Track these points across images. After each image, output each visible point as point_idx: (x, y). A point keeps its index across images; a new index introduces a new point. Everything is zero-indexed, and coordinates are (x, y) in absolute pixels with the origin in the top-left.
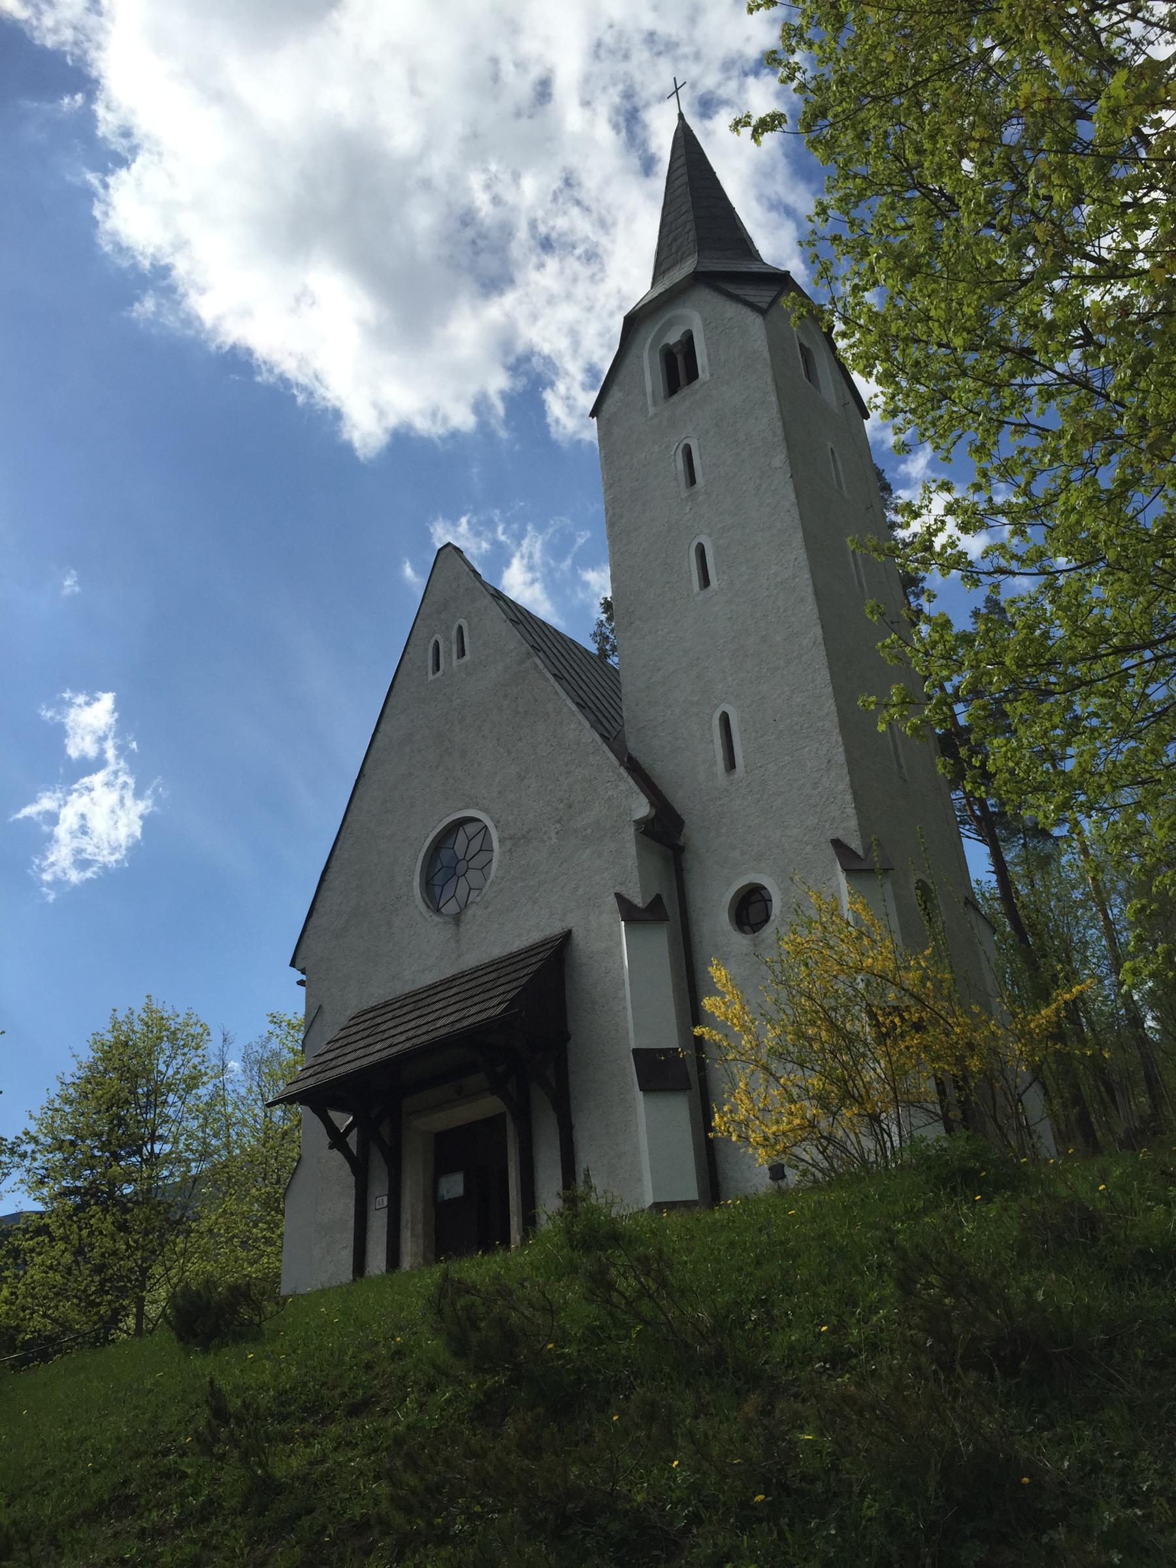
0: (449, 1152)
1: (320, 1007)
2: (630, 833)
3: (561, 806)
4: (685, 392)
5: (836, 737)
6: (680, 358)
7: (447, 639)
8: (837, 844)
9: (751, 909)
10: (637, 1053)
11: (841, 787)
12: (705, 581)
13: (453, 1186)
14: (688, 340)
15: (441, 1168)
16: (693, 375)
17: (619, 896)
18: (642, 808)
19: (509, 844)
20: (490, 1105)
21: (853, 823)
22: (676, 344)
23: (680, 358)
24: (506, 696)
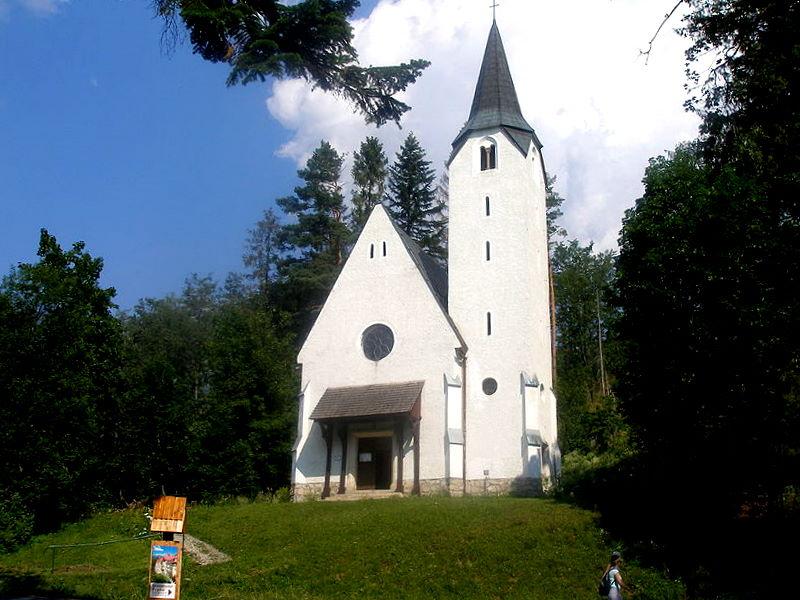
0: (364, 445)
4: (488, 171)
6: (488, 155)
9: (490, 386)
13: (367, 457)
14: (493, 148)
15: (361, 451)
16: (493, 166)
18: (459, 346)
23: (488, 155)
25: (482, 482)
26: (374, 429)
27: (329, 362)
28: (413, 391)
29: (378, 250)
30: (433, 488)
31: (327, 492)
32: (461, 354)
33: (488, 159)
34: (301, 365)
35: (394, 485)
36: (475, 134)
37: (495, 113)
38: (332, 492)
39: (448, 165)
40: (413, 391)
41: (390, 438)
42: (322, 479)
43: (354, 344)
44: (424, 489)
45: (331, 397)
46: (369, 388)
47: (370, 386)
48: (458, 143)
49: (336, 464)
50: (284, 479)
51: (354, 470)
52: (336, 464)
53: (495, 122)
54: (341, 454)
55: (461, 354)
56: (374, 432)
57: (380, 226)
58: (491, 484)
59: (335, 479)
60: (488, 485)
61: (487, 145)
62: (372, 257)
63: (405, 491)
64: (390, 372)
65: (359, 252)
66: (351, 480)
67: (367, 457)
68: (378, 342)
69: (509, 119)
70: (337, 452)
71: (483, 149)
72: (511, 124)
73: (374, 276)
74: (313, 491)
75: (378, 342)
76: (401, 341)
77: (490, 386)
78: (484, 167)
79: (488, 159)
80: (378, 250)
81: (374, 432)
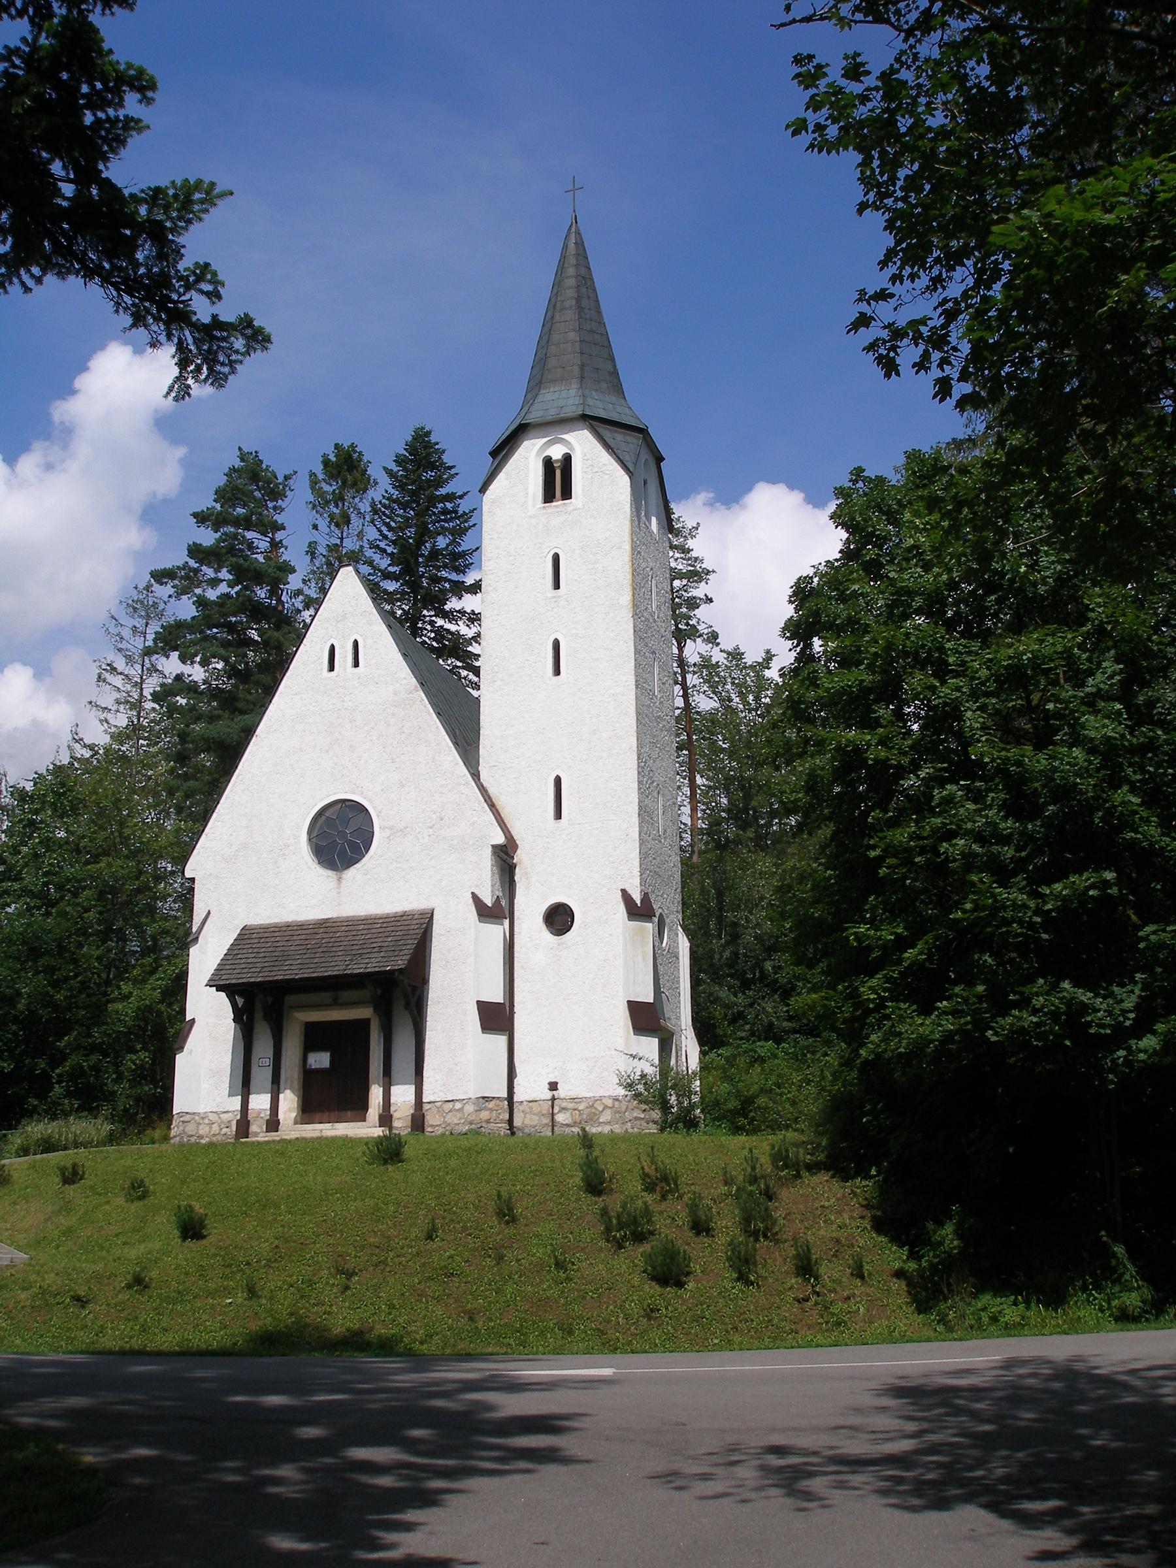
0: (315, 1037)
1: (209, 912)
2: (488, 852)
4: (558, 503)
5: (635, 820)
7: (342, 647)
8: (624, 892)
9: (559, 919)
10: (478, 1002)
14: (567, 459)
16: (567, 494)
17: (473, 893)
18: (500, 839)
19: (388, 832)
20: (364, 1013)
21: (637, 881)
22: (557, 461)
24: (393, 715)
25: (546, 1107)
26: (336, 1003)
27: (248, 874)
28: (417, 933)
29: (344, 657)
30: (452, 1119)
31: (243, 1126)
32: (505, 858)
33: (557, 481)
34: (193, 880)
36: (533, 433)
37: (573, 392)
38: (254, 1128)
39: (483, 489)
40: (417, 933)
42: (236, 1103)
45: (247, 937)
46: (325, 925)
47: (326, 921)
48: (503, 450)
51: (296, 1084)
53: (572, 410)
55: (505, 858)
56: (342, 1008)
58: (563, 1109)
59: (260, 1102)
60: (556, 1109)
62: (331, 668)
63: (396, 1124)
64: (369, 892)
65: (307, 658)
66: (289, 1102)
67: (321, 1060)
68: (341, 835)
69: (599, 404)
70: (263, 1050)
71: (548, 463)
72: (603, 415)
74: (215, 1128)
75: (341, 835)
76: (388, 832)
78: (549, 497)
79: (557, 481)
80: (344, 657)
81: (342, 1008)
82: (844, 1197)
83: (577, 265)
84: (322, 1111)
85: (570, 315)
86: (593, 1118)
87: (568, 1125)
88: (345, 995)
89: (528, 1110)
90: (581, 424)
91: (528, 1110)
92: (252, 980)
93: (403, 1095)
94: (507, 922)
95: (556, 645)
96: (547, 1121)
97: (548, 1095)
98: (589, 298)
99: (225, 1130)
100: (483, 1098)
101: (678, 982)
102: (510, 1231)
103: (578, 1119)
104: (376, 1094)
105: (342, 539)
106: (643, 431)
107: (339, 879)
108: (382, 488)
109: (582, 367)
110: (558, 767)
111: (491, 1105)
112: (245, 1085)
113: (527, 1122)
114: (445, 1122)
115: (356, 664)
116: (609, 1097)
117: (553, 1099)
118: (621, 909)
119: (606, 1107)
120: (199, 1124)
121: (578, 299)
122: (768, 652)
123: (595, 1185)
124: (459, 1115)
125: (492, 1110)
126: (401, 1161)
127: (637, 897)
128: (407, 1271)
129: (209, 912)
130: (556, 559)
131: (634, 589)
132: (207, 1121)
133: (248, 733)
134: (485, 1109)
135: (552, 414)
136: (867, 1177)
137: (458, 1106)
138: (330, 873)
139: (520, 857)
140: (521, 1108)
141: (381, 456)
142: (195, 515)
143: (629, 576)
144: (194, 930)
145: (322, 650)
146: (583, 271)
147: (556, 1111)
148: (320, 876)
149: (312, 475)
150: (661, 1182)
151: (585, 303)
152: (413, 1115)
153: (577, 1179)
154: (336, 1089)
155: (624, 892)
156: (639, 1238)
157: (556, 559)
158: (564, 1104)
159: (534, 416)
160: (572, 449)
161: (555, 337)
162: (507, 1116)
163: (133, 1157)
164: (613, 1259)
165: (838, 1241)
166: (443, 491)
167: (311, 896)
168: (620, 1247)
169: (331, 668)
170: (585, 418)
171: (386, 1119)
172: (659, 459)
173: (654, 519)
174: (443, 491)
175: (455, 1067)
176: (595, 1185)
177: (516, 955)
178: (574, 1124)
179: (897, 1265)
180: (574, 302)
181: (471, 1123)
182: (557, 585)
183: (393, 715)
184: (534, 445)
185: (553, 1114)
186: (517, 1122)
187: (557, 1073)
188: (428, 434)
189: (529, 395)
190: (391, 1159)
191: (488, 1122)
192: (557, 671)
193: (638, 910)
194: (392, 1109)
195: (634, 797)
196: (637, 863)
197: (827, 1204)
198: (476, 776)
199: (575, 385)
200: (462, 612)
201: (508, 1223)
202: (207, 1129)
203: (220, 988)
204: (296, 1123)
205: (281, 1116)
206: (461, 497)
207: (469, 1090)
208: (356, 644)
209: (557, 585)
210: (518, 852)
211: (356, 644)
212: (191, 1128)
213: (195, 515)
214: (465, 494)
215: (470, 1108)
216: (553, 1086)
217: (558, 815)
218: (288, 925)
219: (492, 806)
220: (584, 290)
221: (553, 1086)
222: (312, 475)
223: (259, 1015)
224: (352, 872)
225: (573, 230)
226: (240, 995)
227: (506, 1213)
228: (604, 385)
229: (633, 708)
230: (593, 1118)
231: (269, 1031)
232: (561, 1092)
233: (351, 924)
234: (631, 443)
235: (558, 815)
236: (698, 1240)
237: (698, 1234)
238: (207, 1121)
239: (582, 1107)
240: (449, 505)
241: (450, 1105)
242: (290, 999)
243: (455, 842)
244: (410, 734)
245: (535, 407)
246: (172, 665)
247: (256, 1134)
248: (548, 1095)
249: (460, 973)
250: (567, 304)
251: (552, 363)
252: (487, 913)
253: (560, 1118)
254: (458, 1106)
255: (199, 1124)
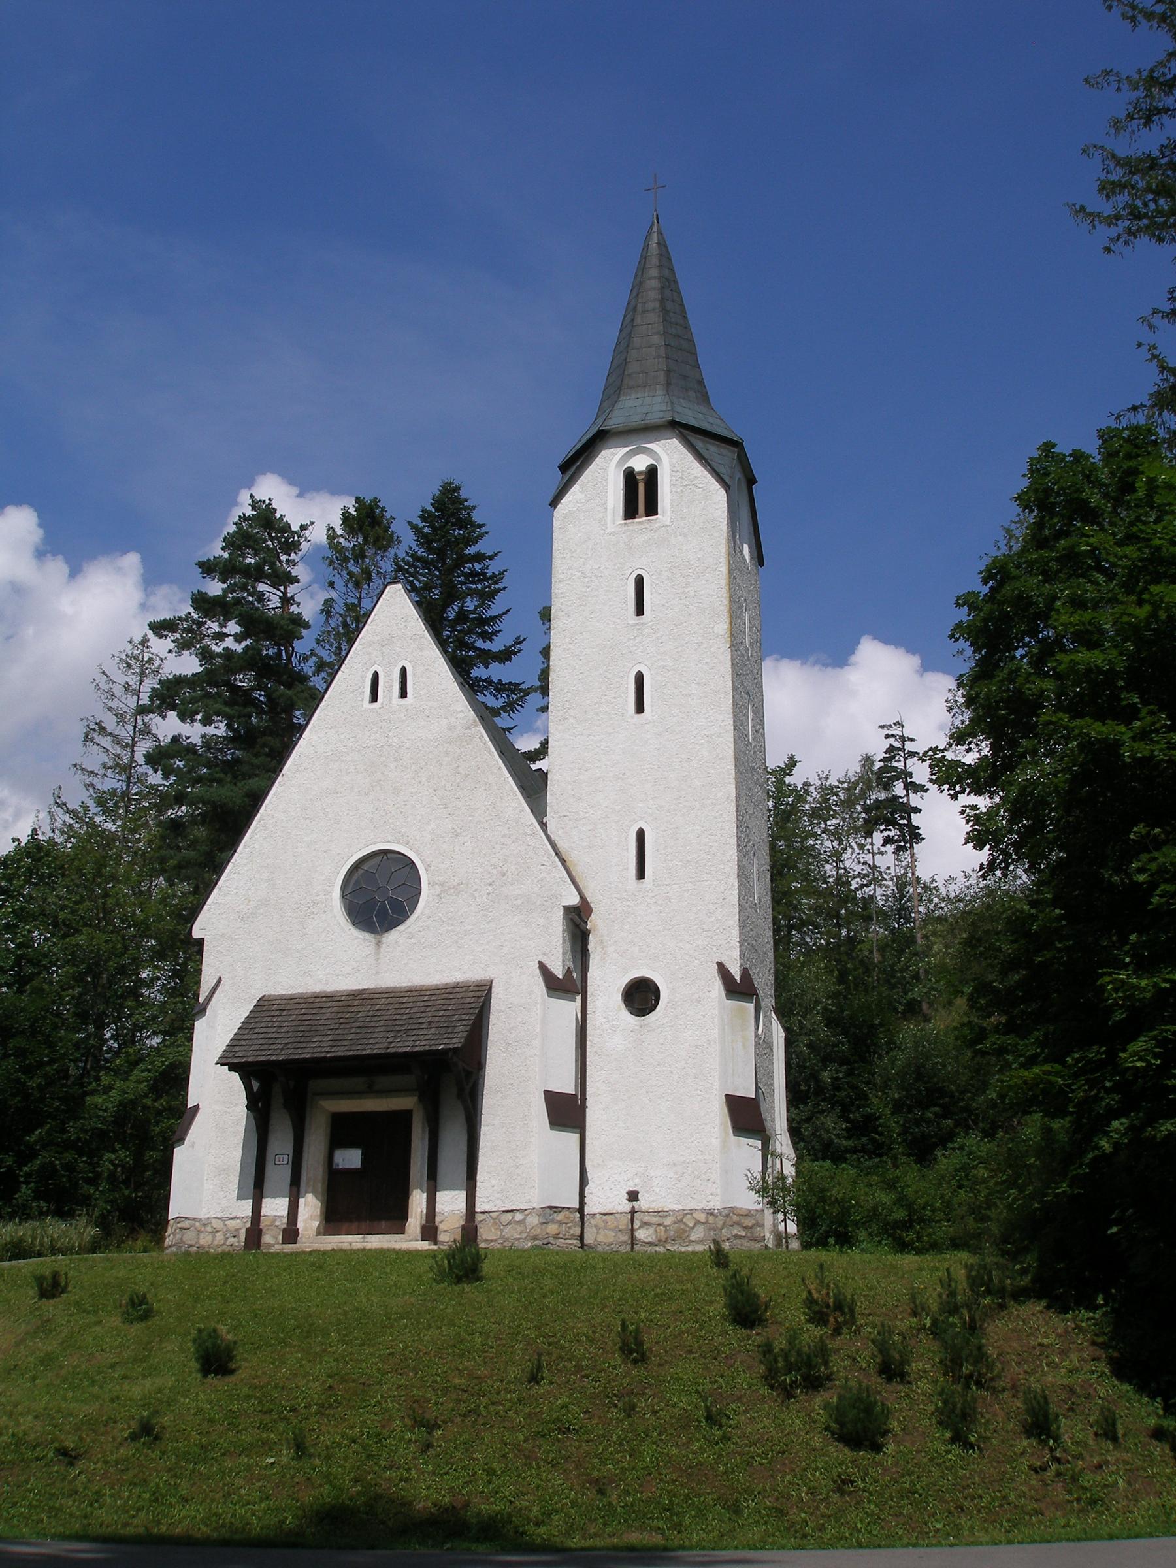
0: (344, 1131)
1: (220, 980)
2: (560, 913)
3: (494, 871)
6: (641, 487)
7: (388, 675)
8: (720, 965)
10: (545, 1092)
11: (731, 922)
12: (640, 708)
13: (350, 1158)
14: (652, 472)
16: (652, 509)
18: (574, 900)
19: (438, 889)
21: (736, 953)
22: (640, 473)
23: (641, 487)
24: (447, 753)
26: (371, 1091)
27: (269, 935)
28: (472, 1006)
30: (512, 1233)
31: (254, 1233)
32: (578, 922)
33: (641, 495)
35: (414, 1223)
37: (658, 399)
38: (267, 1239)
39: (554, 503)
40: (472, 1006)
41: (404, 1117)
42: (246, 1208)
43: (328, 893)
44: (487, 1235)
45: (267, 1010)
47: (362, 992)
48: (575, 463)
49: (279, 1173)
50: (142, 1203)
51: (320, 1187)
52: (279, 1173)
54: (289, 1148)
55: (578, 922)
56: (379, 1094)
57: (395, 624)
58: (645, 1224)
59: (275, 1207)
60: (637, 1224)
61: (640, 464)
62: (374, 698)
63: (442, 1237)
64: (411, 960)
65: (345, 690)
66: (310, 1208)
67: (350, 1158)
71: (630, 477)
72: (694, 423)
73: (382, 737)
74: (220, 1237)
75: (380, 893)
76: (438, 889)
77: (641, 996)
78: (630, 512)
79: (641, 495)
81: (379, 1094)
82: (1066, 1332)
83: (660, 266)
84: (351, 1221)
85: (654, 318)
86: (682, 1235)
87: (650, 1244)
88: (383, 1081)
89: (602, 1224)
90: (669, 432)
91: (602, 1224)
92: (274, 1058)
93: (451, 1203)
94: (579, 998)
95: (640, 679)
96: (625, 1238)
97: (626, 1206)
98: (673, 301)
99: (231, 1240)
100: (551, 1208)
101: (772, 1078)
102: (638, 1372)
103: (663, 1236)
104: (418, 1201)
105: (360, 599)
106: (736, 444)
107: (379, 944)
108: (407, 543)
109: (668, 372)
110: (641, 818)
111: (560, 1217)
112: (257, 1185)
113: (601, 1238)
114: (502, 1237)
115: (403, 694)
116: (702, 1210)
117: (633, 1212)
118: (718, 986)
119: (698, 1222)
120: (200, 1231)
121: (662, 301)
122: (791, 758)
123: (746, 1312)
124: (519, 1228)
125: (560, 1223)
126: (479, 1279)
127: (736, 972)
128: (506, 1424)
129: (220, 980)
130: (640, 582)
131: (731, 617)
132: (209, 1229)
133: (256, 800)
134: (553, 1221)
135: (635, 420)
136: (1094, 1307)
137: (519, 1217)
138: (367, 935)
139: (595, 922)
140: (592, 1221)
141: (405, 509)
142: (201, 565)
143: (726, 602)
144: (201, 1000)
145: (363, 678)
146: (666, 272)
147: (636, 1226)
148: (356, 940)
149: (330, 528)
150: (832, 1312)
151: (669, 305)
152: (463, 1227)
153: (719, 1306)
154: (368, 1198)
155: (720, 965)
156: (814, 1383)
157: (640, 582)
158: (647, 1218)
159: (615, 421)
160: (658, 459)
161: (637, 341)
162: (578, 1232)
163: (126, 1266)
164: (781, 1412)
165: (1072, 1390)
166: (471, 551)
167: (341, 961)
168: (790, 1396)
169: (374, 698)
170: (676, 427)
171: (430, 1231)
172: (751, 481)
173: (746, 547)
174: (471, 551)
175: (515, 1172)
176: (746, 1312)
177: (589, 1038)
178: (660, 1242)
179: (1153, 1422)
180: (657, 304)
181: (535, 1238)
182: (640, 611)
183: (447, 753)
184: (614, 454)
185: (632, 1230)
186: (588, 1239)
187: (637, 1181)
188: (457, 489)
189: (605, 404)
190: (467, 1276)
191: (556, 1237)
192: (640, 708)
193: (738, 988)
194: (438, 1219)
195: (733, 854)
196: (735, 932)
197: (1045, 1341)
198: (544, 826)
199: (660, 391)
200: (489, 681)
201: (635, 1361)
202: (209, 1238)
203: (233, 1067)
204: (318, 1234)
205: (300, 1225)
206: (491, 558)
207: (532, 1197)
208: (404, 671)
209: (640, 611)
210: (592, 916)
211: (404, 671)
212: (189, 1238)
213: (201, 565)
214: (496, 554)
215: (533, 1220)
216: (633, 1196)
217: (641, 874)
218: (316, 996)
219: (563, 862)
220: (667, 292)
221: (633, 1196)
222: (330, 528)
223: (277, 1100)
224: (394, 936)
225: (655, 229)
226: (257, 1079)
227: (633, 1349)
228: (692, 394)
229: (730, 752)
230: (682, 1235)
231: (290, 1123)
232: (643, 1203)
233: (392, 996)
234: (725, 457)
235: (641, 874)
236: (890, 1387)
237: (889, 1380)
238: (209, 1229)
239: (668, 1221)
240: (477, 567)
241: (509, 1216)
242: (315, 1085)
243: (519, 902)
244: (467, 776)
245: (616, 413)
246: (168, 726)
247: (270, 1245)
248: (626, 1206)
249: (522, 1058)
250: (650, 306)
251: (633, 367)
252: (556, 986)
253: (642, 1234)
254: (519, 1217)
255: (200, 1231)
